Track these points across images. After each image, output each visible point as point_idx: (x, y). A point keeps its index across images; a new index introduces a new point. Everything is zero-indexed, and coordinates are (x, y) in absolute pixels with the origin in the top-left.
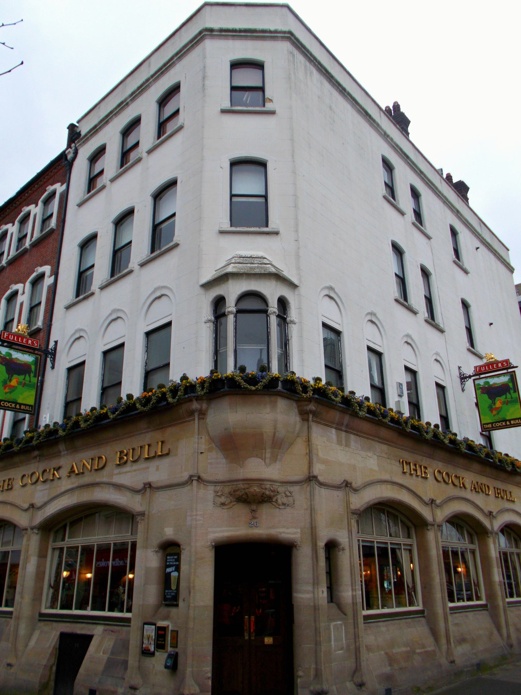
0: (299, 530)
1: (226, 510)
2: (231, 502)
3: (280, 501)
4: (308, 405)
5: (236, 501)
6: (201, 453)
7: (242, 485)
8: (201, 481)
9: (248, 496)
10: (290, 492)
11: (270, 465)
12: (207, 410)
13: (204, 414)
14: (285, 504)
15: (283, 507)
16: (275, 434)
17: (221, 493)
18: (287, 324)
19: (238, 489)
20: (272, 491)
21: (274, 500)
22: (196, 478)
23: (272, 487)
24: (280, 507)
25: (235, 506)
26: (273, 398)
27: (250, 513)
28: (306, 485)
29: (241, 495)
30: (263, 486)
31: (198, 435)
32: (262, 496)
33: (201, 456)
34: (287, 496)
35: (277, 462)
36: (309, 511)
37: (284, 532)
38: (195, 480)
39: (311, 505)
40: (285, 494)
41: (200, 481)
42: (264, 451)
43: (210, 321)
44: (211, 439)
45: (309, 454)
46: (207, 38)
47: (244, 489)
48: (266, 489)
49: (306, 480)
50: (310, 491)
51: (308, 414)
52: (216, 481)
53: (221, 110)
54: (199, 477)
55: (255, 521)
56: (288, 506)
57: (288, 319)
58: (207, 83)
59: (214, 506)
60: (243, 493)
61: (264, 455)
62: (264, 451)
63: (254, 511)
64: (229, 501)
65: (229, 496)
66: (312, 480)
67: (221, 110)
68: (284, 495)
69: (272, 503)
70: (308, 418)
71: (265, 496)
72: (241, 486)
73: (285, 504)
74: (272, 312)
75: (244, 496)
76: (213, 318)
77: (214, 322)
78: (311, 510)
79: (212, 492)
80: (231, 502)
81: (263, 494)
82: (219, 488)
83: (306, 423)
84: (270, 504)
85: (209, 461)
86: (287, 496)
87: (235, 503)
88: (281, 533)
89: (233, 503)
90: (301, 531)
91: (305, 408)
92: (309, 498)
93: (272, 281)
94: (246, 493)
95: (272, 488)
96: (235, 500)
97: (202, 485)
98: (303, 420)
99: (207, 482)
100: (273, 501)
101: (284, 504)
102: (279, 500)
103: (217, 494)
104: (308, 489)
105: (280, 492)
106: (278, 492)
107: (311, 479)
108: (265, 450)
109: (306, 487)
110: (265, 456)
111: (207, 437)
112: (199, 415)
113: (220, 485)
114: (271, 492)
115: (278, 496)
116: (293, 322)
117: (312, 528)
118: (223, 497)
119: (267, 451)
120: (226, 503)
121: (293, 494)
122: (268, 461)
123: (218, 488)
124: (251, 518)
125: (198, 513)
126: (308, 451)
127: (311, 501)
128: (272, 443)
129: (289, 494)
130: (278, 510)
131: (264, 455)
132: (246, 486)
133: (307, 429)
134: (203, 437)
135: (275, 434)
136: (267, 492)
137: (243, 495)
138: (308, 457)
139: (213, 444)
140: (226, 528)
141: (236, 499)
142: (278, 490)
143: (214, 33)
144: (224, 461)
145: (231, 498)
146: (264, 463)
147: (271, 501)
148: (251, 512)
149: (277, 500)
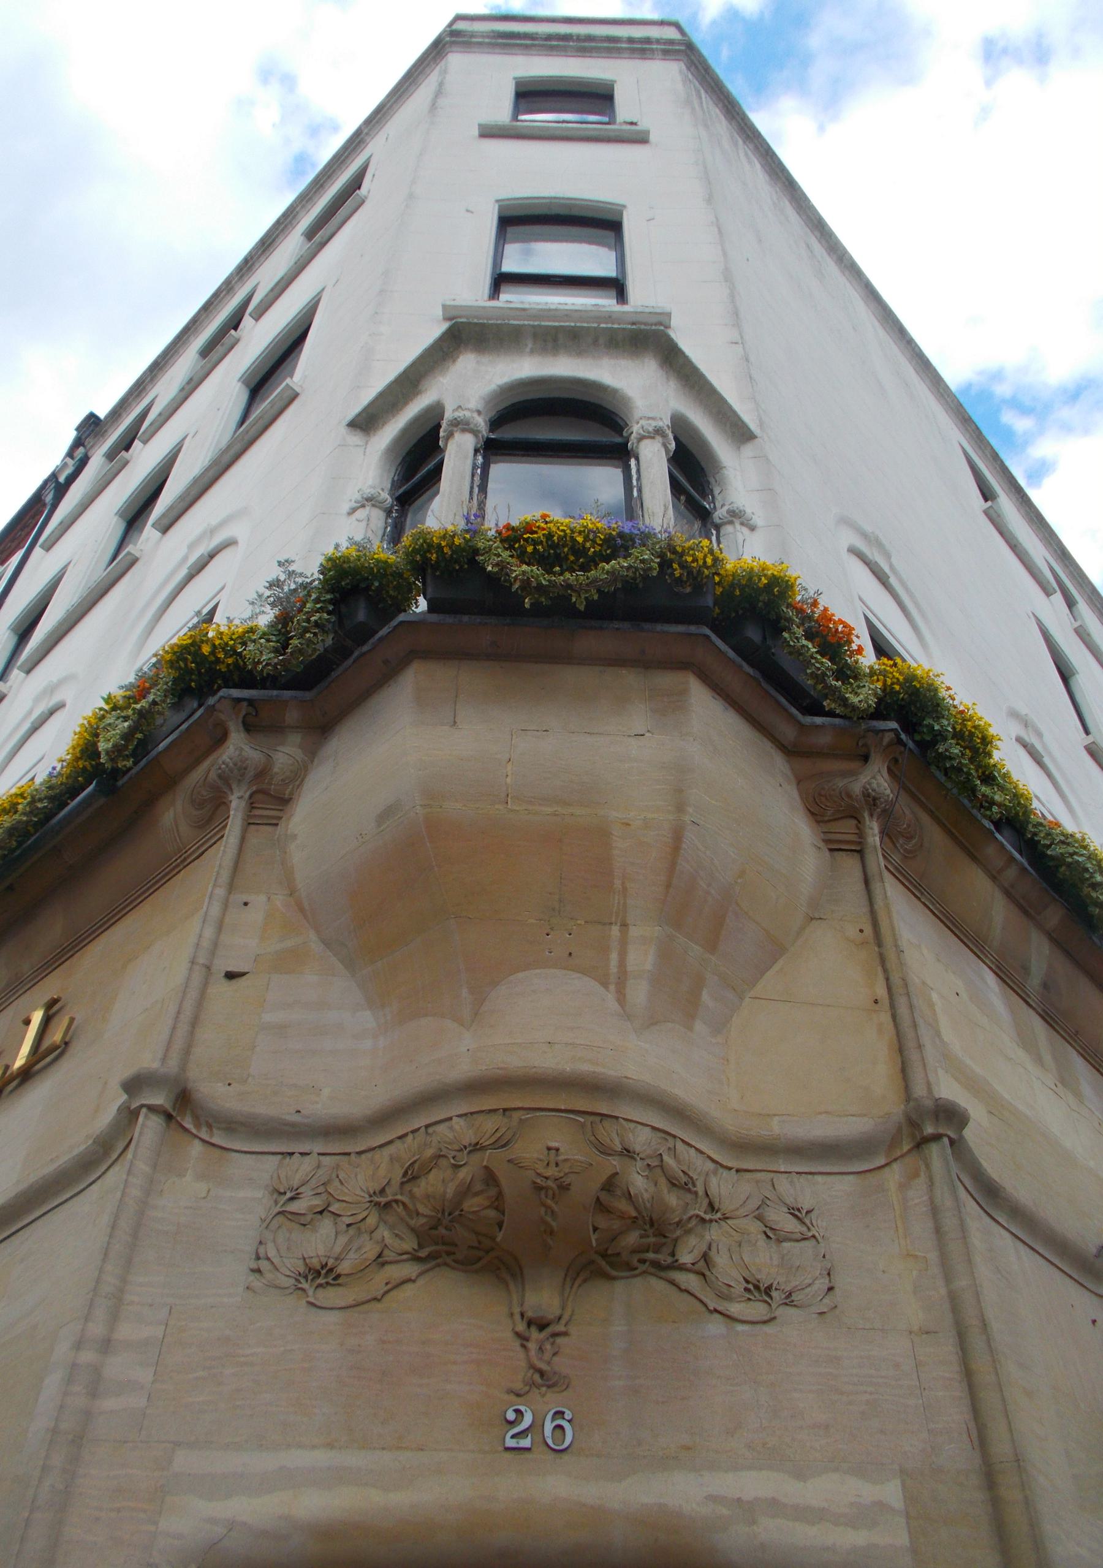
0: (891, 1492)
1: (333, 1317)
2: (380, 1261)
3: (725, 1268)
4: (853, 773)
5: (418, 1259)
6: (231, 976)
7: (458, 1124)
8: (198, 1126)
9: (498, 1203)
10: (795, 1212)
11: (652, 1022)
12: (298, 776)
13: (284, 801)
14: (768, 1290)
15: (757, 1310)
16: (678, 836)
17: (318, 1202)
18: (718, 528)
19: (439, 1157)
20: (673, 1184)
21: (686, 1258)
22: (159, 1099)
23: (673, 1150)
24: (735, 1309)
25: (409, 1290)
26: (666, 680)
27: (516, 1344)
28: (894, 1176)
29: (450, 1190)
30: (611, 1135)
31: (231, 887)
32: (600, 1206)
33: (221, 989)
34: (771, 1234)
35: (699, 1026)
36: (948, 1348)
37: (774, 1506)
38: (151, 1108)
39: (954, 1300)
40: (759, 1218)
41: (188, 1124)
42: (615, 931)
43: (370, 500)
44: (302, 910)
45: (893, 1006)
46: (454, 49)
47: (477, 1148)
48: (628, 1153)
49: (894, 1142)
50: (935, 1211)
51: (859, 821)
52: (297, 1118)
53: (481, 126)
54: (184, 1098)
55: (553, 1401)
56: (788, 1300)
57: (719, 514)
58: (441, 102)
59: (256, 1282)
60: (463, 1174)
61: (614, 957)
62: (615, 931)
63: (542, 1327)
64: (370, 1250)
65: (372, 1220)
66: (937, 1138)
67: (481, 126)
68: (755, 1228)
69: (681, 1277)
70: (861, 834)
71: (623, 1205)
72: (462, 1131)
73: (768, 1290)
74: (651, 429)
75: (472, 1204)
76: (386, 497)
77: (389, 512)
78: (962, 1337)
79: (259, 1194)
80: (380, 1261)
81: (610, 1185)
82: (306, 1166)
83: (850, 863)
84: (657, 1285)
85: (268, 1017)
86: (771, 1234)
87: (409, 1269)
88: (748, 1509)
89: (396, 1272)
90: (910, 1498)
91: (840, 783)
92: (933, 1256)
93: (646, 360)
94: (490, 1177)
95: (668, 1160)
96: (409, 1244)
97: (197, 1148)
98: (834, 847)
99: (233, 1125)
100: (682, 1268)
101: (759, 1290)
102: (721, 1260)
103: (294, 1207)
104: (918, 1194)
105: (727, 1206)
106: (712, 1207)
107: (929, 1130)
108: (624, 925)
109: (903, 1187)
110: (622, 963)
111: (279, 900)
112: (252, 806)
113: (318, 1147)
114: (663, 1181)
115: (714, 1233)
116: (736, 515)
117: (990, 1478)
118: (326, 1226)
119: (634, 932)
120: (344, 1267)
121: (820, 1224)
122: (639, 993)
123: (300, 1170)
124: (518, 1386)
125: (125, 1331)
126: (881, 991)
127: (948, 1277)
128: (668, 886)
129: (790, 1225)
130: (715, 1327)
131: (614, 957)
132: (490, 1125)
133: (860, 886)
134: (259, 900)
135: (678, 836)
136: (638, 1182)
137: (465, 1191)
138: (885, 1018)
139: (312, 936)
140: (321, 1458)
141: (422, 1236)
142: (713, 1190)
143: (474, 40)
144: (367, 1019)
145: (385, 1233)
146: (612, 1004)
147: (663, 1258)
148: (523, 1338)
149: (705, 1257)
